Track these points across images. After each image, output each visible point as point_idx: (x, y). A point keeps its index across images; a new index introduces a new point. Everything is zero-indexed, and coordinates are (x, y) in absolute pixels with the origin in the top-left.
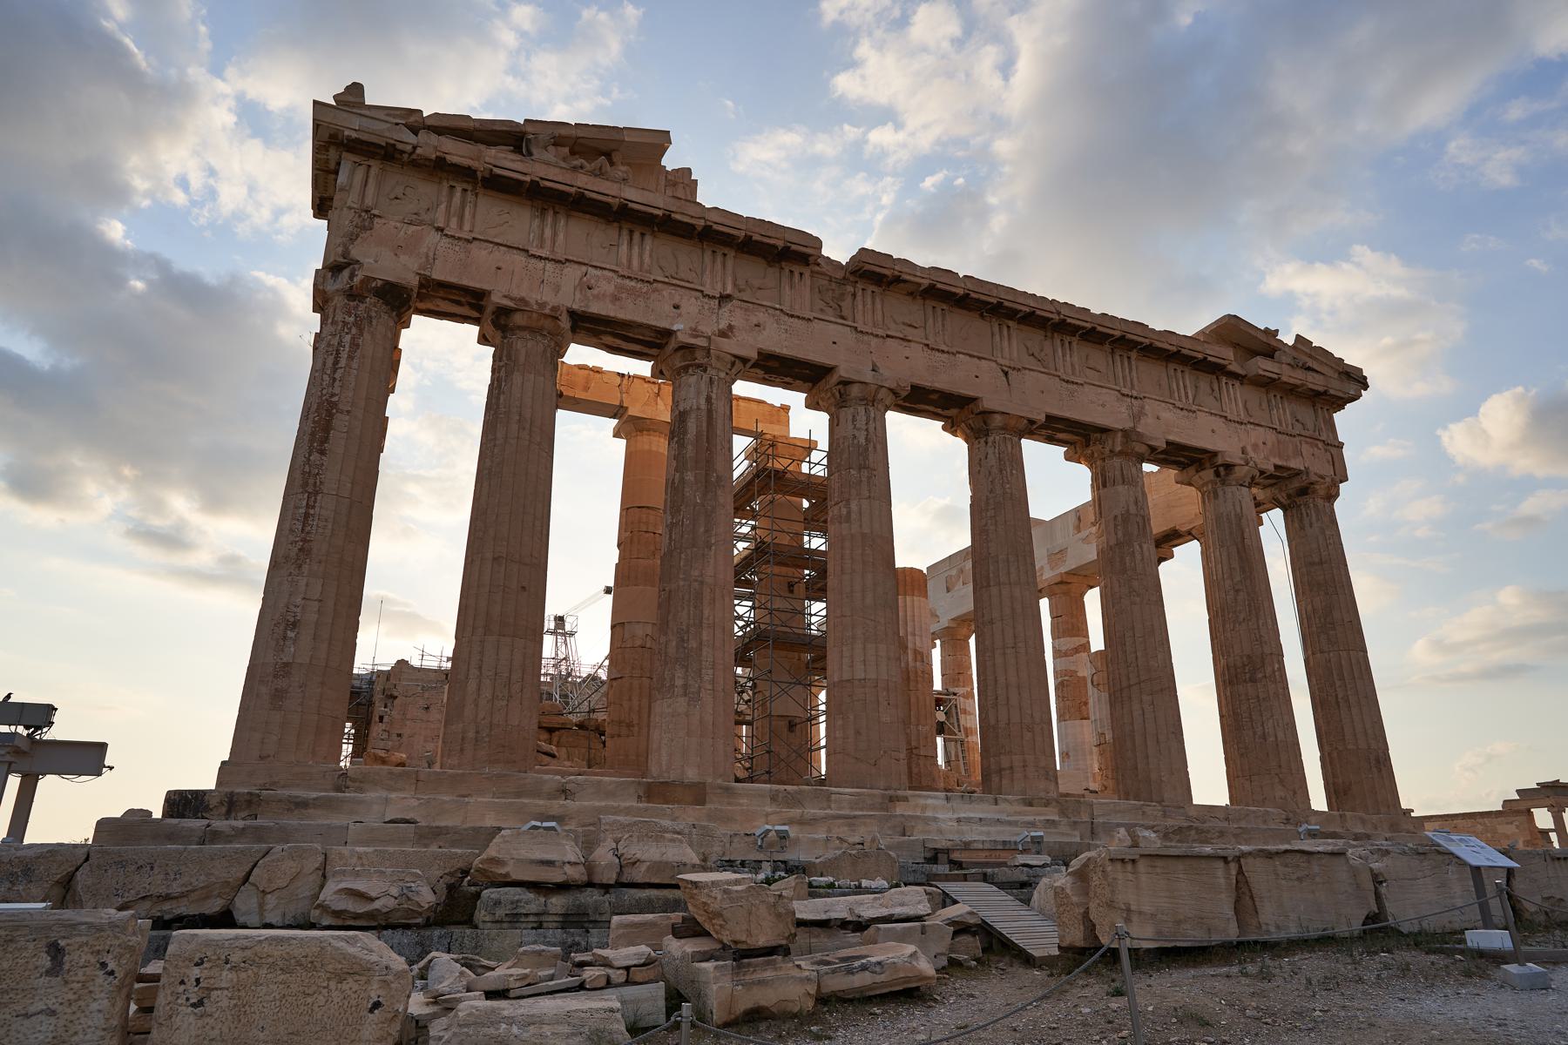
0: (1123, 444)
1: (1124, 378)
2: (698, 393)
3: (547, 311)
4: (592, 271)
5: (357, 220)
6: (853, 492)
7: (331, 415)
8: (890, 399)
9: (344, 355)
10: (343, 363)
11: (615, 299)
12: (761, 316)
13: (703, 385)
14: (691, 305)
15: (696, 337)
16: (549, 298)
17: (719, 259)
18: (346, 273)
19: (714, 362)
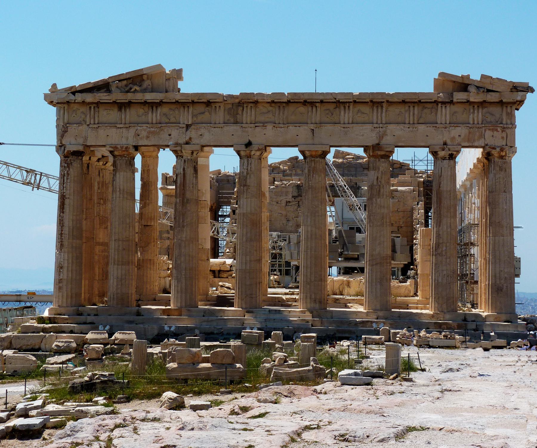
0: (373, 152)
1: (377, 118)
2: (181, 167)
3: (124, 149)
4: (139, 128)
5: (63, 129)
6: (242, 196)
7: (64, 200)
8: (258, 153)
9: (65, 178)
10: (65, 180)
11: (148, 137)
12: (202, 131)
13: (182, 164)
14: (175, 133)
15: (176, 147)
16: (124, 142)
17: (186, 109)
18: (63, 148)
19: (184, 154)
